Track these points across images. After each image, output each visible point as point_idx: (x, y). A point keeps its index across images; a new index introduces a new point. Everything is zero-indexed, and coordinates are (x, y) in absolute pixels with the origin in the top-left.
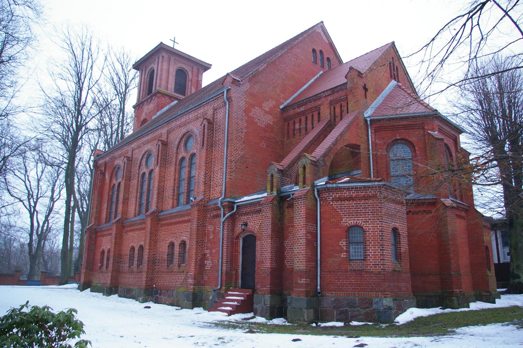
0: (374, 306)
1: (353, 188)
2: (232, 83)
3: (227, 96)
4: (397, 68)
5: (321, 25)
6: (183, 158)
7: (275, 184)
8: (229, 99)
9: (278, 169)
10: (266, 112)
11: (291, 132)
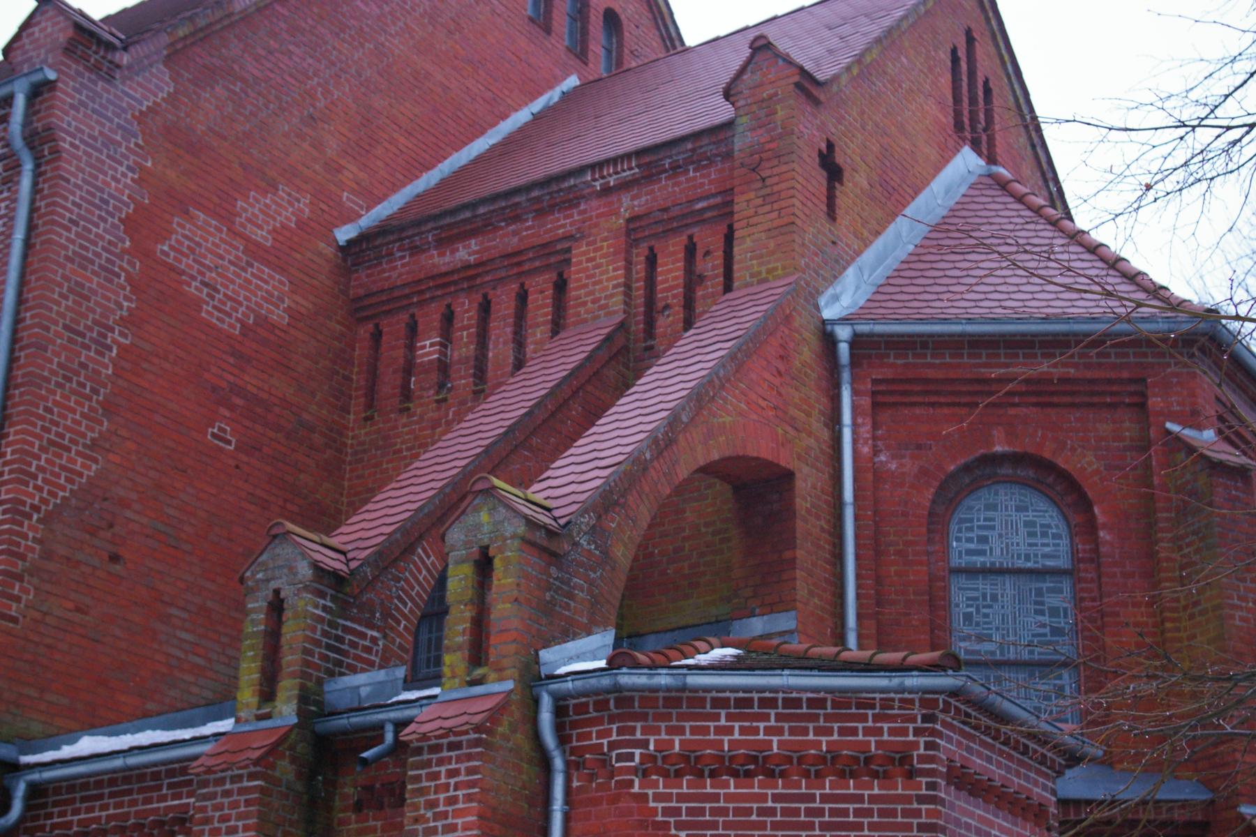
1: (771, 703)
2: (69, 50)
3: (27, 123)
4: (988, 91)
7: (290, 659)
8: (40, 140)
9: (316, 566)
10: (255, 251)
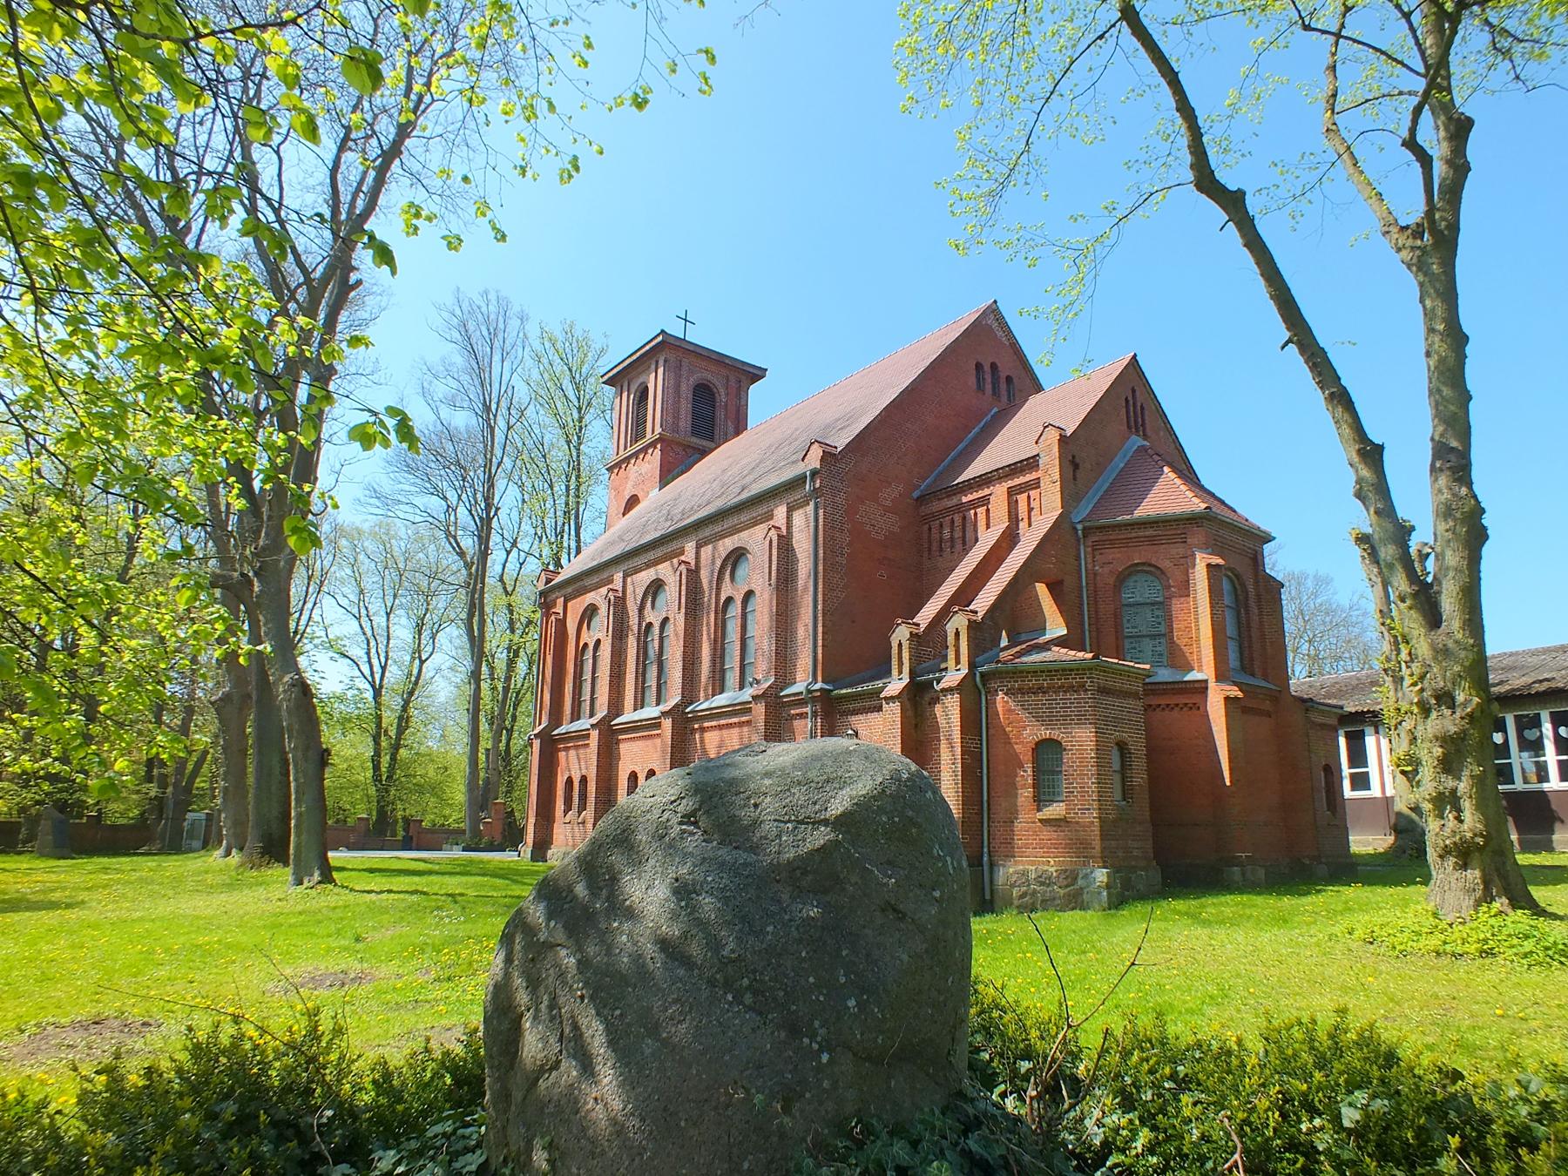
0: (1080, 882)
4: (1142, 408)
5: (993, 311)
6: (729, 600)
10: (887, 510)
11: (935, 545)
